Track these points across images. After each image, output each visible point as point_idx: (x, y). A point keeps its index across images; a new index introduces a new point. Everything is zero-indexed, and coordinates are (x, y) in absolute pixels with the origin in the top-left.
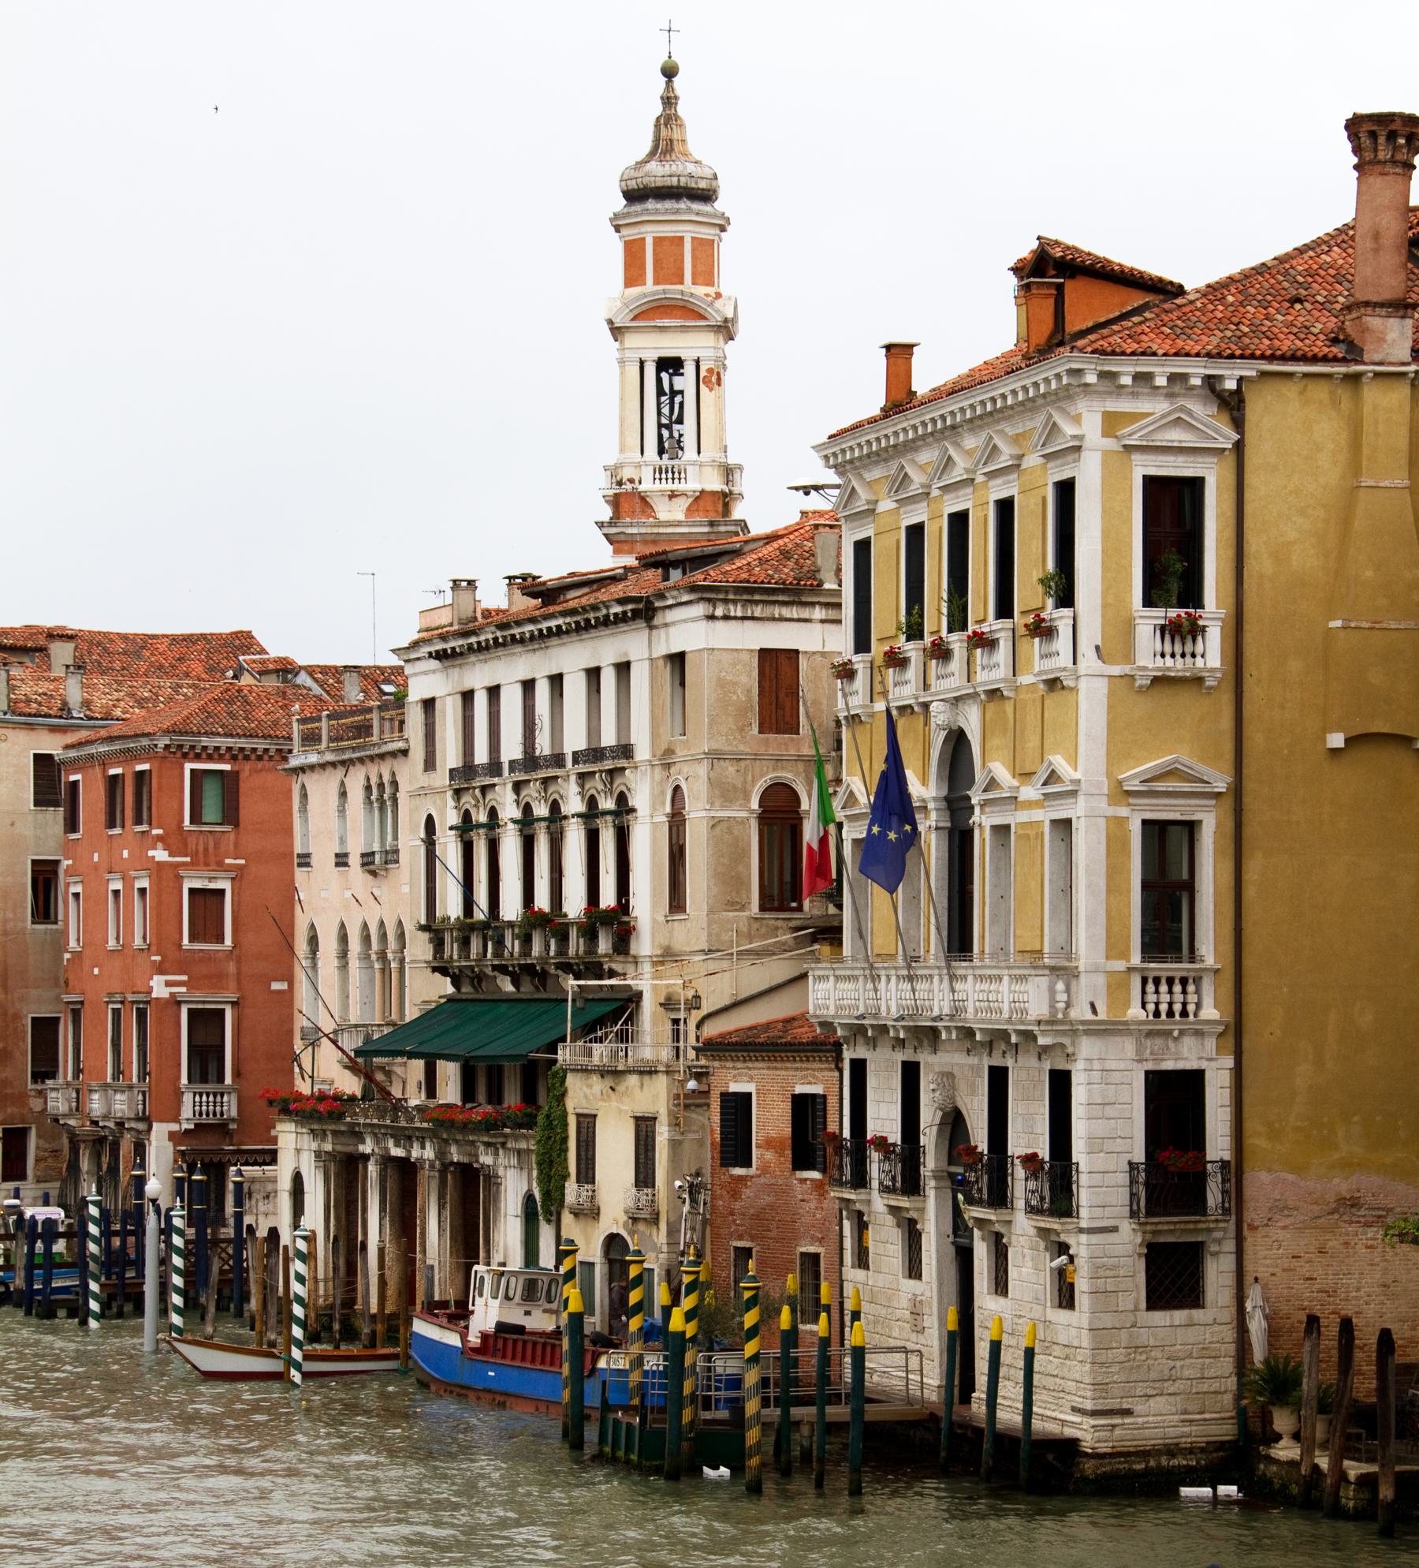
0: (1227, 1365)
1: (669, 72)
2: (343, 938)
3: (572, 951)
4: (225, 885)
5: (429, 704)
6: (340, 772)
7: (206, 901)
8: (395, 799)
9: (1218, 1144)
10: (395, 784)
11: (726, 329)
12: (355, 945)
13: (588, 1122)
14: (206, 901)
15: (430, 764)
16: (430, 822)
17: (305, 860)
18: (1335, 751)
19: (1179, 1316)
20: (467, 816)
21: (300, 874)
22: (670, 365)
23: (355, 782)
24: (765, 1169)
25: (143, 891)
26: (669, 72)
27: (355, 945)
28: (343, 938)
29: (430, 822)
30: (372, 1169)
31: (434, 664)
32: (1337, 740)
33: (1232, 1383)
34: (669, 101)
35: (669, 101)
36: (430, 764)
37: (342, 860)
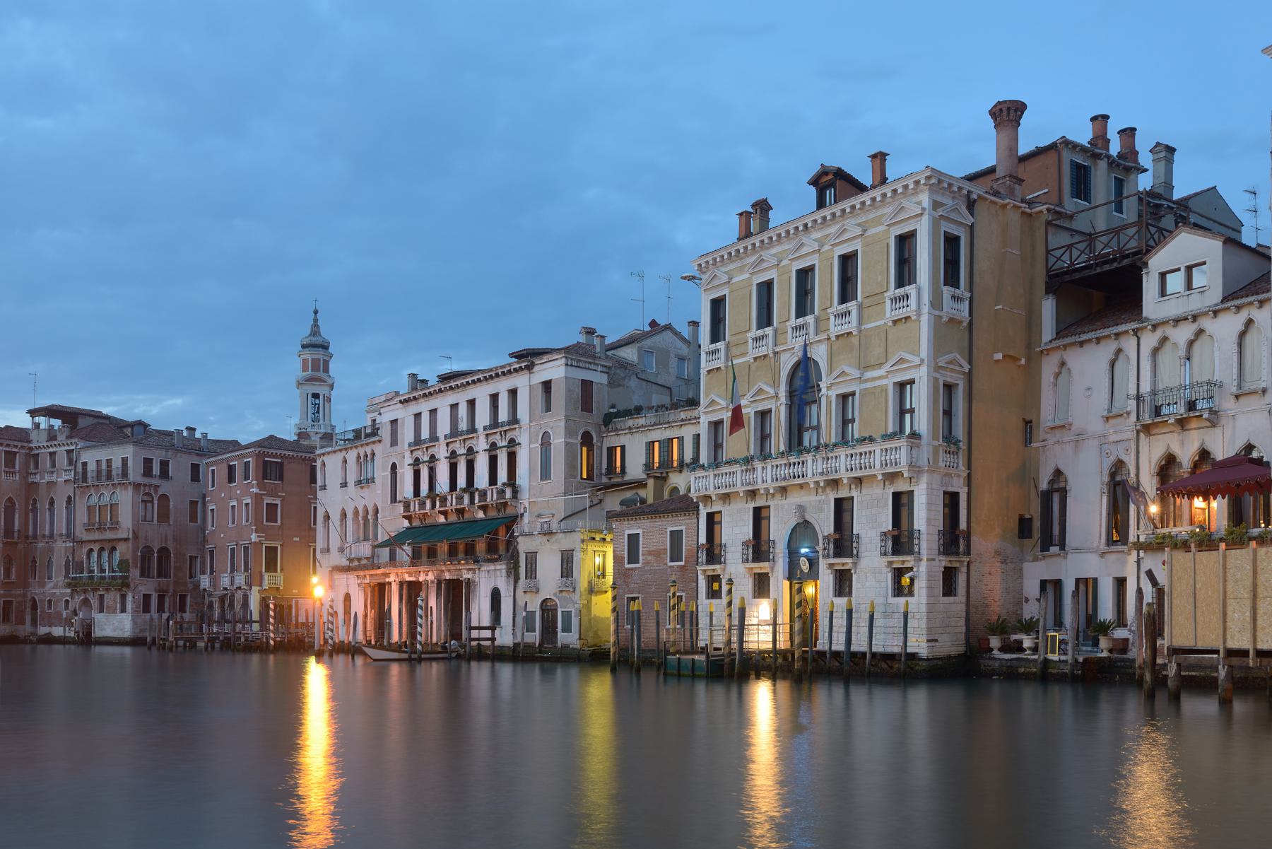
0: (963, 622)
1: (316, 312)
2: (344, 515)
3: (489, 499)
4: (278, 502)
5: (394, 422)
6: (344, 453)
7: (272, 508)
8: (373, 459)
9: (963, 525)
10: (373, 454)
11: (332, 387)
12: (350, 516)
13: (532, 559)
14: (272, 508)
15: (394, 442)
16: (394, 466)
17: (324, 487)
18: (997, 361)
19: (951, 599)
20: (417, 460)
21: (320, 494)
22: (316, 396)
23: (352, 456)
24: (647, 563)
25: (247, 505)
26: (316, 312)
27: (350, 516)
28: (344, 515)
29: (394, 466)
30: (395, 588)
31: (400, 405)
32: (999, 356)
33: (964, 629)
34: (316, 320)
35: (316, 320)
36: (394, 442)
37: (344, 485)
